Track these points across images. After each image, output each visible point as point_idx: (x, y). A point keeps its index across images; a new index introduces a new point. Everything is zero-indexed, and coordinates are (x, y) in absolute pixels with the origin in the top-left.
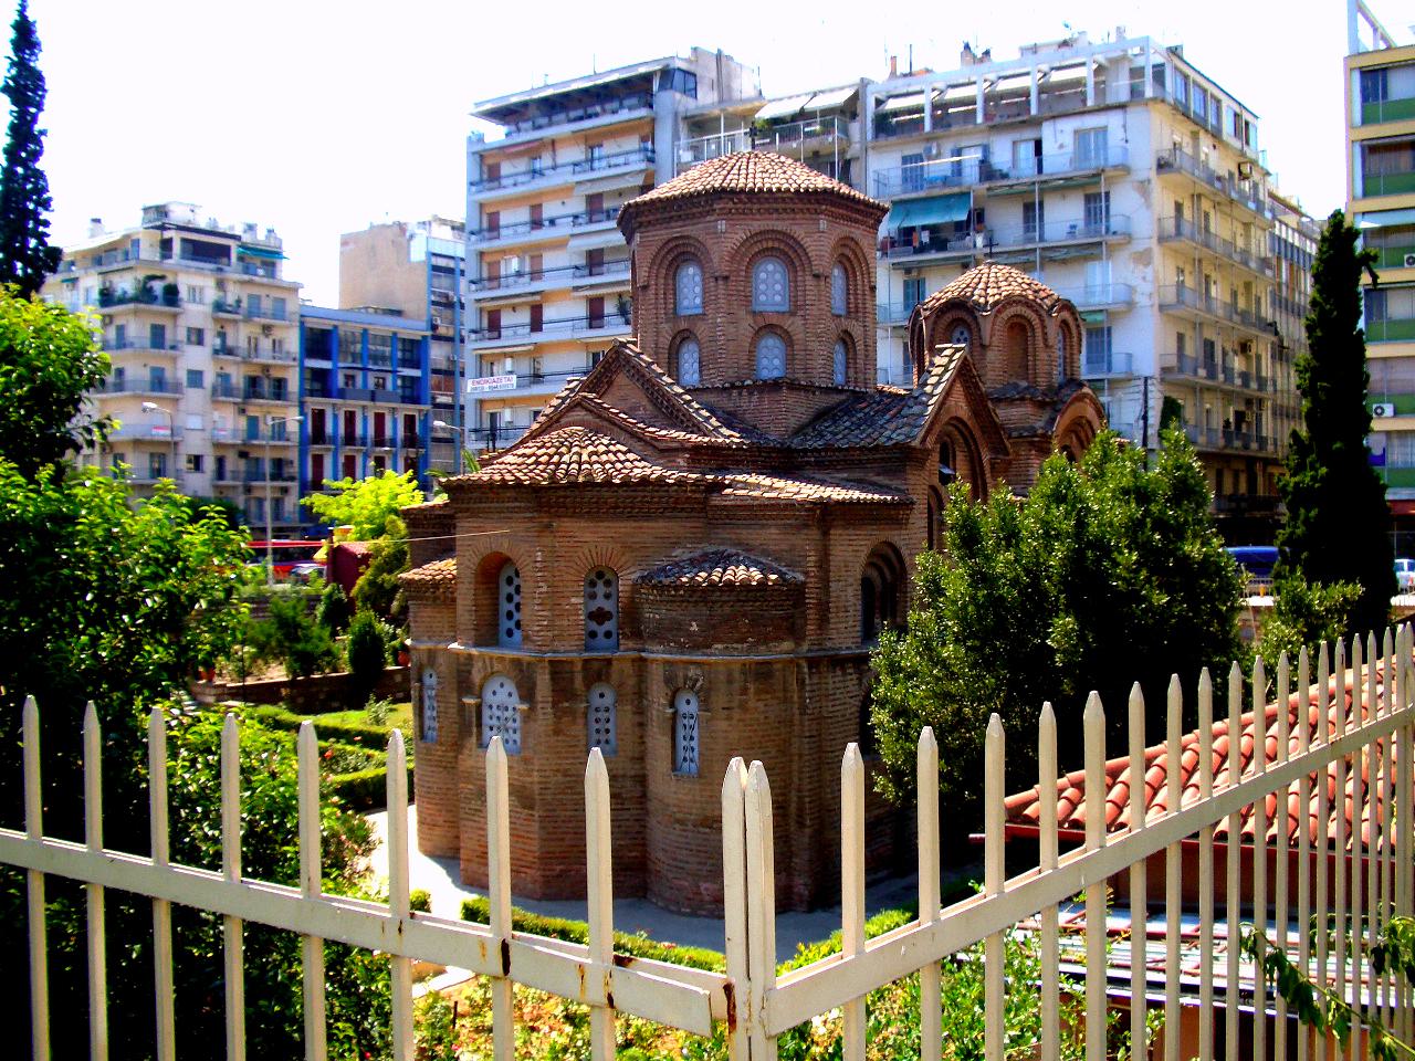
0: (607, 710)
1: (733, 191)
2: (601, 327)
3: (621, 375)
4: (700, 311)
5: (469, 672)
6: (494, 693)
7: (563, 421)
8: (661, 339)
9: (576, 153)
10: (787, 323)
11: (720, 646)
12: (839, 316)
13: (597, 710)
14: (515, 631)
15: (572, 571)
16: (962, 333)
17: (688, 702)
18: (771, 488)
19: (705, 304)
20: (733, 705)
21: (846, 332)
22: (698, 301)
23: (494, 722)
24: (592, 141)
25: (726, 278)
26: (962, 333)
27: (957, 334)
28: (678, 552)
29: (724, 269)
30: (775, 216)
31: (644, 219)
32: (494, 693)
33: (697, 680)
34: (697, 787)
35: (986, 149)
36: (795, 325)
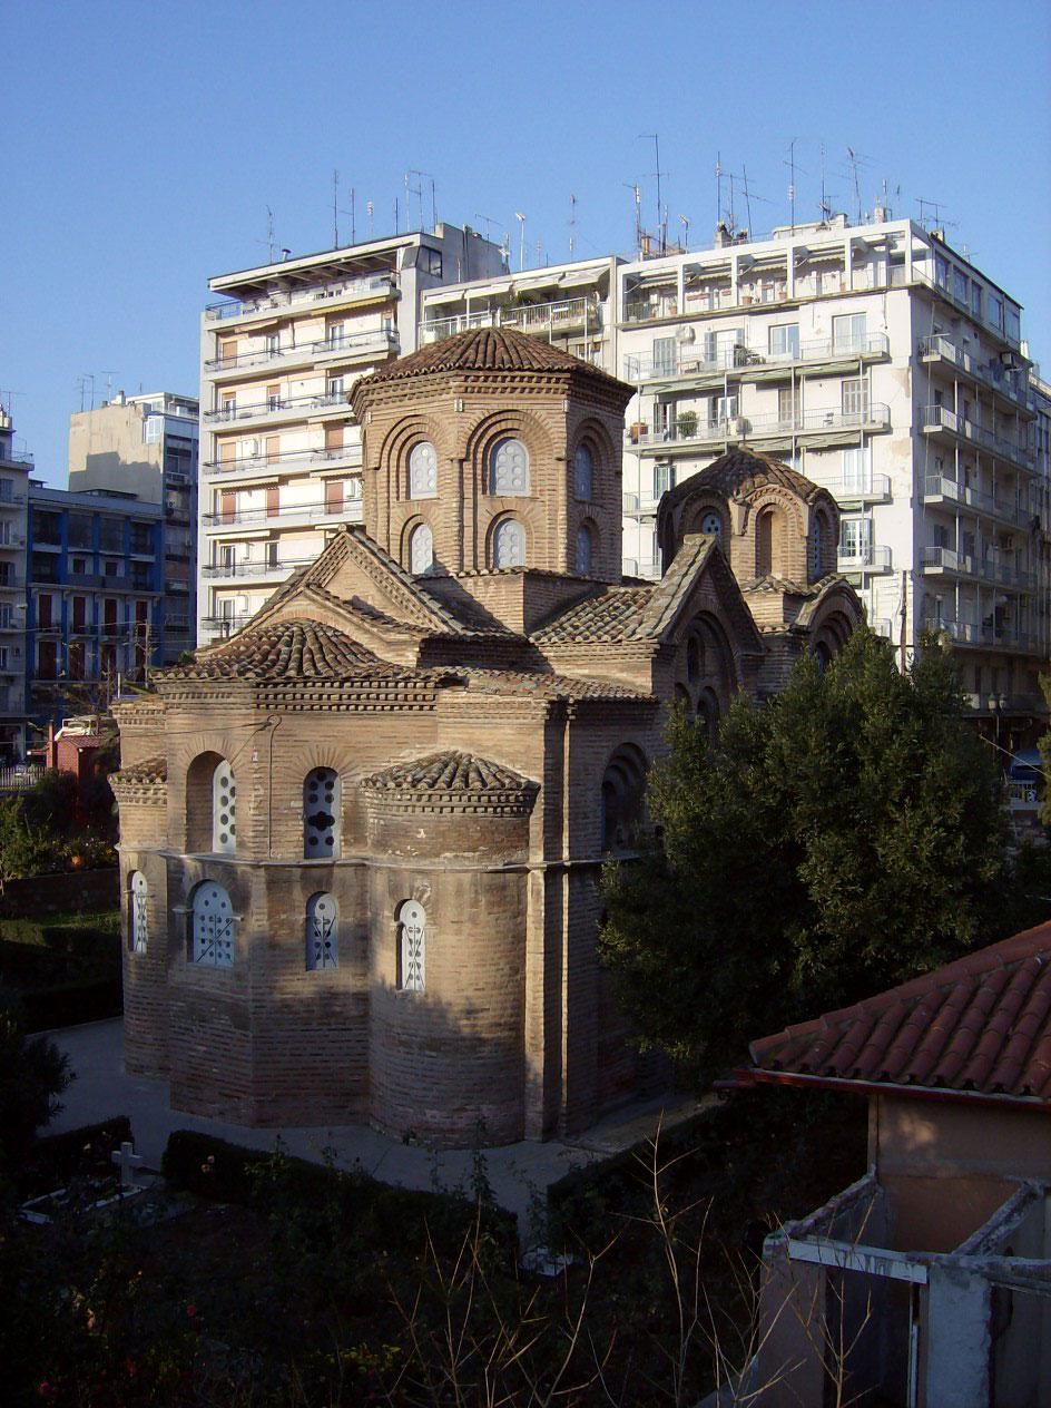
4: (435, 495)
6: (207, 903)
9: (313, 331)
11: (448, 854)
12: (583, 503)
16: (713, 522)
21: (589, 519)
22: (433, 484)
23: (207, 935)
24: (333, 317)
26: (713, 522)
27: (707, 524)
31: (375, 396)
32: (207, 903)
33: (424, 892)
35: (741, 332)
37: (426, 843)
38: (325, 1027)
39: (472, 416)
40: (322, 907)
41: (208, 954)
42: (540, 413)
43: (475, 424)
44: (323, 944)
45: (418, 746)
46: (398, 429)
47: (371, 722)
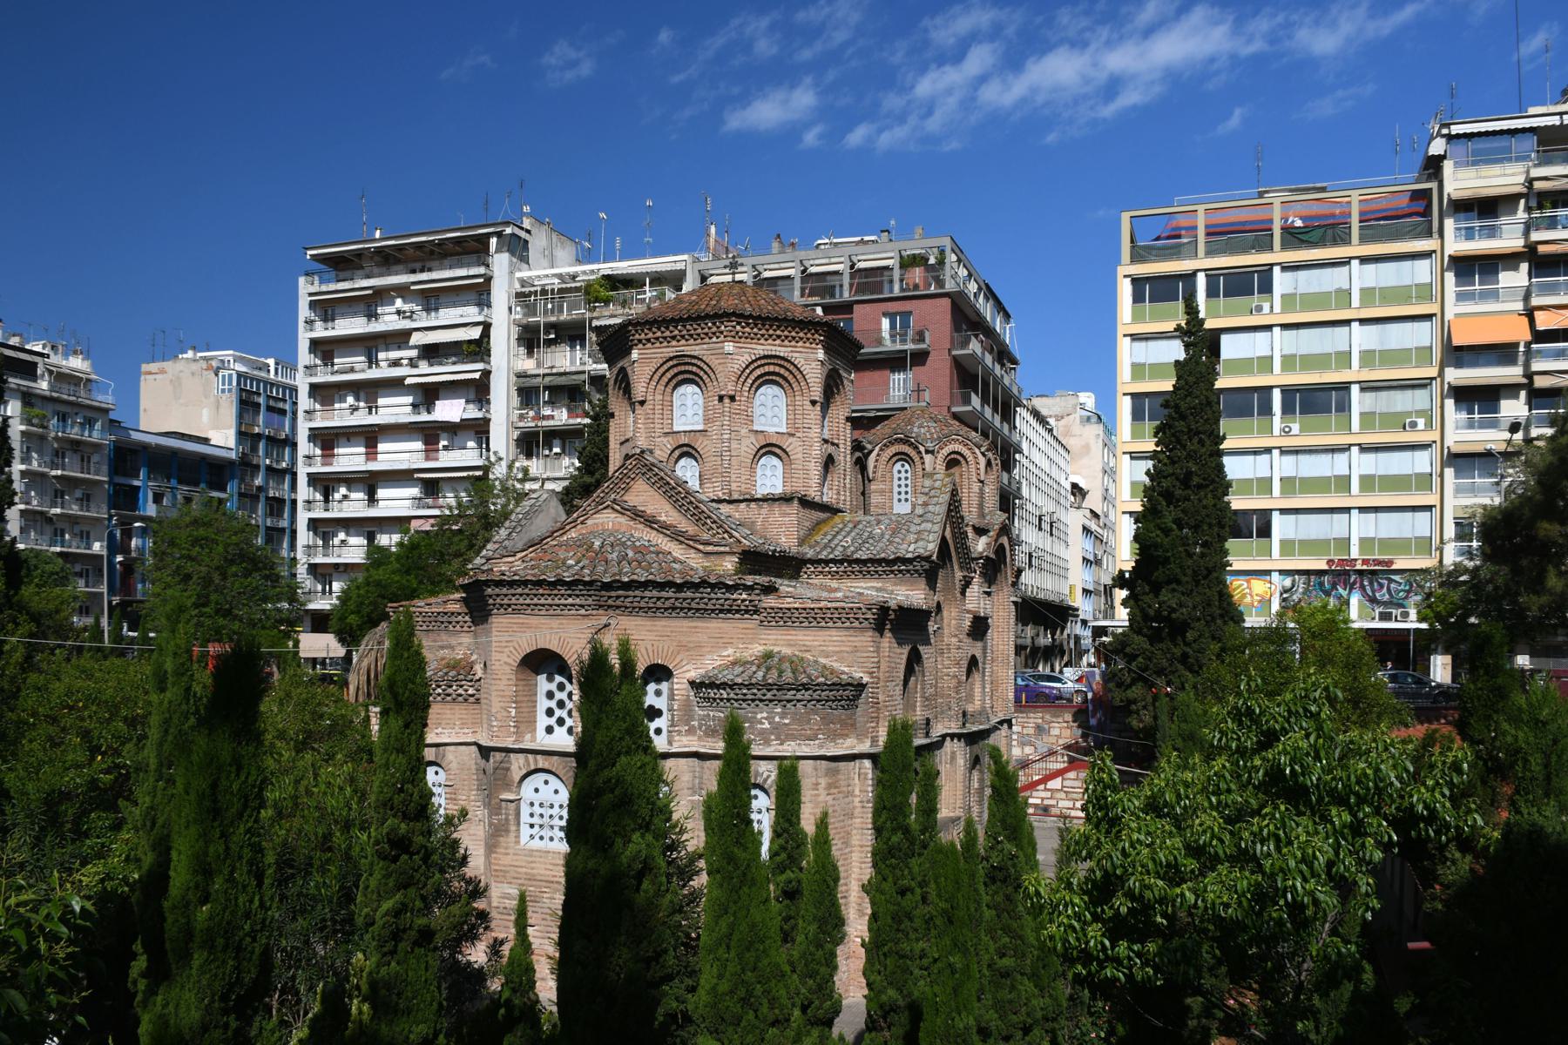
1: (741, 316)
2: (437, 459)
3: (641, 481)
4: (700, 427)
5: (508, 769)
6: (537, 790)
7: (589, 522)
10: (786, 443)
14: (556, 728)
18: (878, 590)
19: (707, 420)
23: (536, 820)
25: (732, 398)
29: (730, 389)
30: (778, 342)
32: (537, 790)
36: (792, 445)
41: (537, 838)
42: (799, 359)
46: (666, 367)
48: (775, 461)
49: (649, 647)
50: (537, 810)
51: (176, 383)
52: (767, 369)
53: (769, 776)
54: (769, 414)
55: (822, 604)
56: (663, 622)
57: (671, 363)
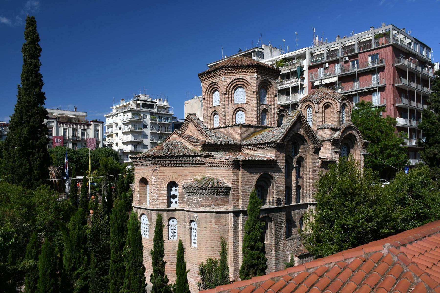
0: (175, 226)
1: (226, 67)
3: (191, 124)
4: (219, 105)
6: (143, 220)
8: (208, 114)
11: (203, 207)
13: (172, 226)
15: (163, 183)
16: (310, 109)
17: (195, 225)
20: (207, 226)
23: (143, 229)
26: (310, 109)
28: (196, 177)
32: (143, 220)
34: (196, 252)
37: (197, 204)
38: (174, 256)
39: (228, 81)
40: (173, 221)
43: (229, 83)
44: (173, 232)
45: (200, 175)
46: (209, 87)
47: (186, 168)
48: (242, 113)
49: (175, 176)
50: (144, 226)
51: (192, 105)
52: (237, 83)
53: (196, 218)
54: (240, 98)
55: (219, 160)
56: (174, 168)
57: (211, 85)
